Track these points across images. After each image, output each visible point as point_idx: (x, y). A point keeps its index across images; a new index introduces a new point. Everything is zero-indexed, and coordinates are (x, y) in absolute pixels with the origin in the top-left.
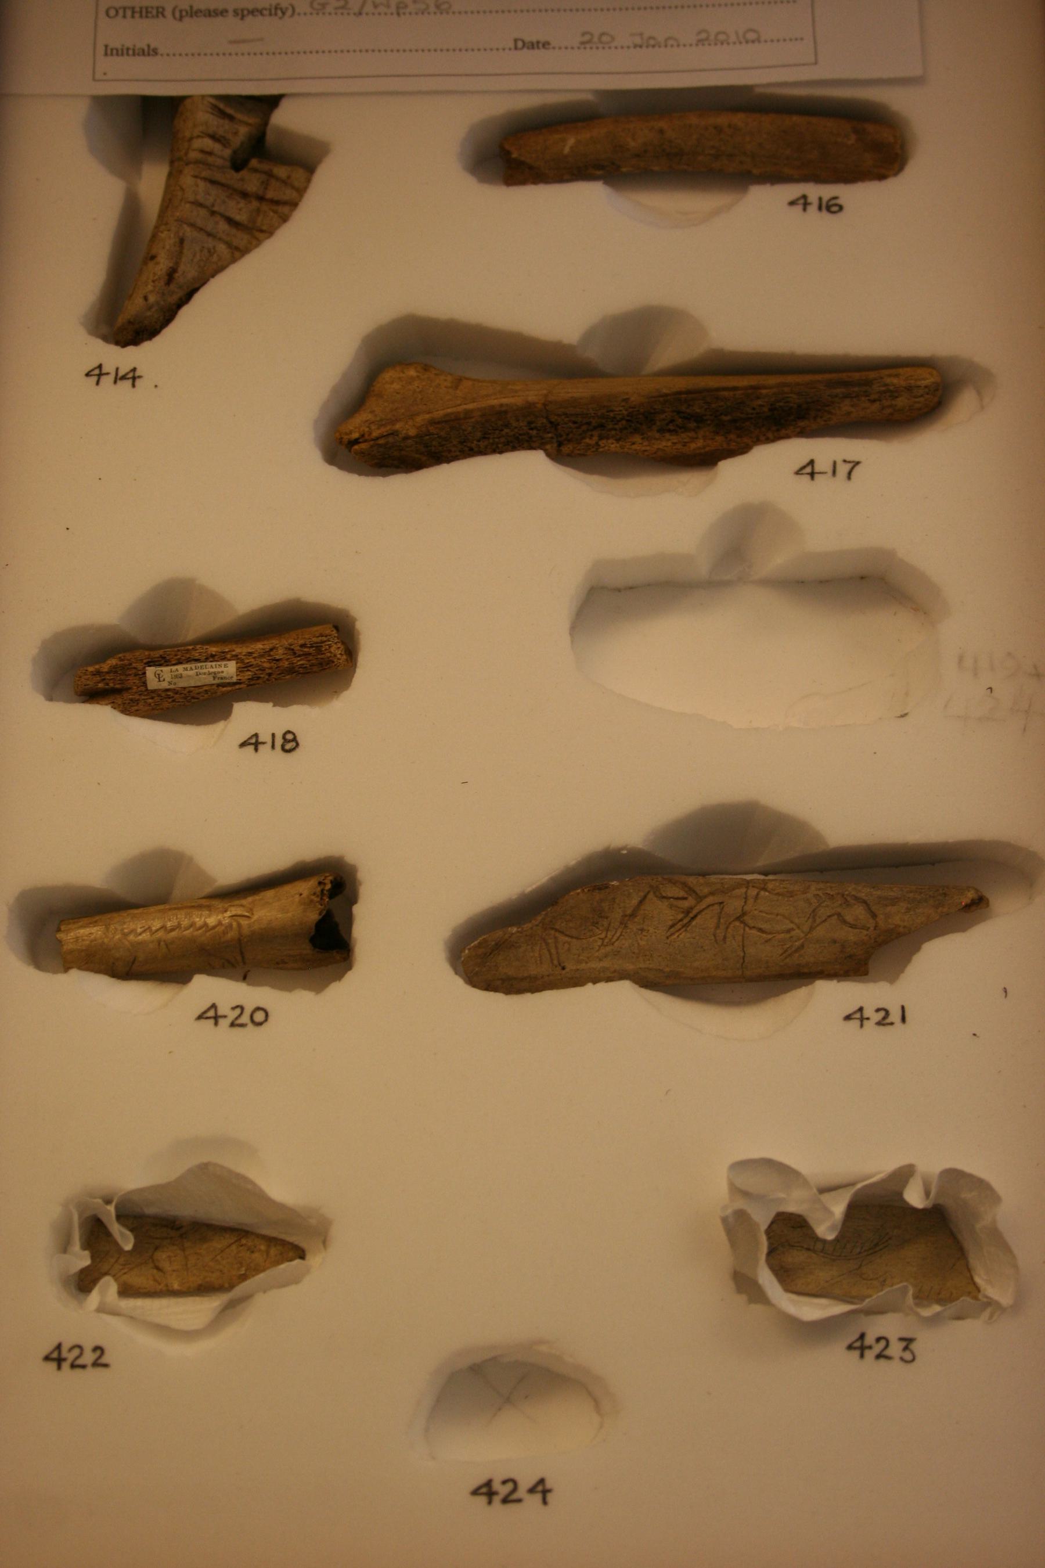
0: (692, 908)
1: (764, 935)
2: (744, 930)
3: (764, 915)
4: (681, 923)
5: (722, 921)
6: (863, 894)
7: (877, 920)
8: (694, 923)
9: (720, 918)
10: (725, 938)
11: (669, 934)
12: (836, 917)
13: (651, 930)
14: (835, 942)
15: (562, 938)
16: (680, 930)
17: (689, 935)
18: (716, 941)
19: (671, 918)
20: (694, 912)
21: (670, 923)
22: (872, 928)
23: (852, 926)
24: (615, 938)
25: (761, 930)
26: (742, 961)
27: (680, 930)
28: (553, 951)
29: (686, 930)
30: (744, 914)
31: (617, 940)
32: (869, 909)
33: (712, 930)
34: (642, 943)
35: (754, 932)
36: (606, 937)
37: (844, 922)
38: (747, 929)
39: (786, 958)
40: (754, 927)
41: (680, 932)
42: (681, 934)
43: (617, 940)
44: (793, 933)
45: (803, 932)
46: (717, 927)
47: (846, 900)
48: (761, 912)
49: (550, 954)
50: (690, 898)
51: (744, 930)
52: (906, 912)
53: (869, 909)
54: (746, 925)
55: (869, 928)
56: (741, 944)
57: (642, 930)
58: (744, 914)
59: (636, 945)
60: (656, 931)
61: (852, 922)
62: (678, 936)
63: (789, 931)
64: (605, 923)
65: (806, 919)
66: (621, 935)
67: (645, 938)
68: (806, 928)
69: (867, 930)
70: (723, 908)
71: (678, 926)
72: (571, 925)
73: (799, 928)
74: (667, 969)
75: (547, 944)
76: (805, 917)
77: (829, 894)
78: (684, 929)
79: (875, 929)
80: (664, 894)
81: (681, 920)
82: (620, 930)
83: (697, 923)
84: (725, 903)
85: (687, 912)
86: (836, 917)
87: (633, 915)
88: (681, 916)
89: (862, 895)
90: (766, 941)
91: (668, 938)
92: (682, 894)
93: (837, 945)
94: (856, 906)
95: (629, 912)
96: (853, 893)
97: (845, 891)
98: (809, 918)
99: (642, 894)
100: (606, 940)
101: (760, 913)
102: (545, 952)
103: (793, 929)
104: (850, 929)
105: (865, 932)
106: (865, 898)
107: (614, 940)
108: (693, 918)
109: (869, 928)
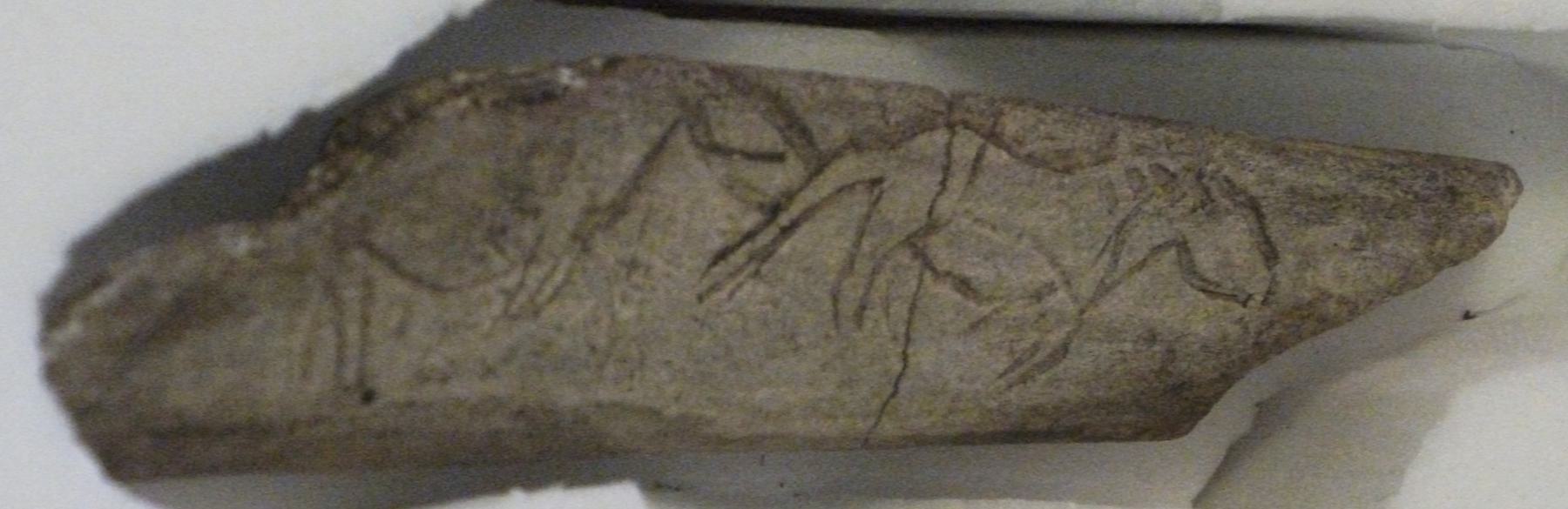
0: (790, 196)
1: (972, 305)
2: (921, 281)
3: (987, 231)
4: (748, 246)
5: (866, 245)
6: (1252, 177)
7: (1278, 269)
8: (785, 249)
9: (861, 234)
10: (859, 317)
11: (707, 282)
12: (1173, 252)
13: (659, 264)
14: (1152, 338)
15: (390, 286)
16: (739, 270)
17: (762, 290)
18: (836, 315)
19: (725, 225)
20: (795, 210)
21: (717, 243)
22: (1259, 298)
23: (1210, 290)
24: (548, 290)
25: (964, 286)
26: (890, 390)
27: (739, 270)
28: (353, 332)
29: (757, 273)
30: (932, 226)
31: (551, 299)
32: (1263, 229)
33: (831, 278)
34: (627, 313)
35: (946, 292)
36: (521, 285)
37: (1189, 269)
38: (928, 275)
39: (1010, 386)
40: (948, 274)
41: (740, 278)
42: (740, 286)
43: (551, 299)
44: (1051, 301)
45: (1075, 299)
46: (849, 266)
47: (1207, 191)
48: (976, 220)
49: (341, 346)
50: (792, 160)
51: (921, 281)
52: (1355, 249)
53: (1263, 229)
54: (928, 264)
55: (1250, 297)
56: (902, 329)
57: (632, 265)
58: (932, 226)
59: (605, 322)
60: (671, 269)
61: (1211, 275)
62: (732, 294)
63: (1038, 297)
64: (528, 232)
65: (1095, 253)
66: (567, 281)
67: (637, 296)
68: (1086, 288)
69: (1244, 304)
70: (879, 198)
71: (739, 257)
72: (425, 233)
73: (1068, 283)
74: (673, 411)
75: (338, 303)
76: (1092, 247)
77: (1166, 170)
78: (752, 268)
79: (1265, 302)
80: (718, 137)
81: (750, 236)
82: (566, 262)
83: (794, 249)
84: (885, 185)
85: (774, 210)
86: (1173, 252)
87: (618, 210)
88: (751, 220)
89: (1247, 180)
90: (974, 326)
91: (700, 298)
92: (769, 139)
93: (1157, 348)
94: (1230, 218)
95: (607, 195)
96: (1227, 171)
97: (1207, 164)
98: (1103, 250)
99: (655, 131)
100: (522, 298)
101: (976, 228)
102: (328, 333)
103: (1051, 288)
104: (1202, 296)
105: (1239, 311)
106: (1255, 191)
107: (541, 299)
108: (787, 231)
109: (1250, 297)
